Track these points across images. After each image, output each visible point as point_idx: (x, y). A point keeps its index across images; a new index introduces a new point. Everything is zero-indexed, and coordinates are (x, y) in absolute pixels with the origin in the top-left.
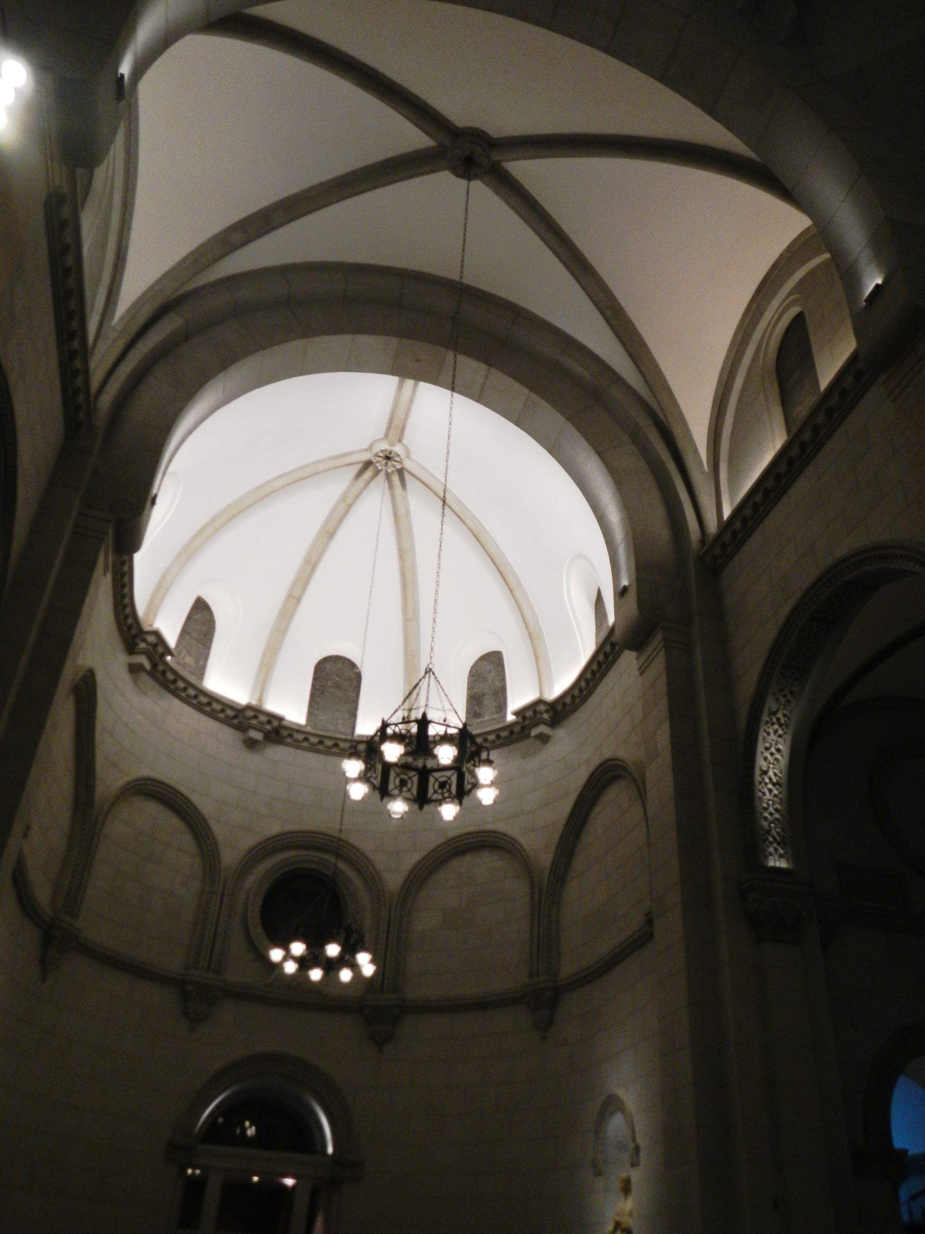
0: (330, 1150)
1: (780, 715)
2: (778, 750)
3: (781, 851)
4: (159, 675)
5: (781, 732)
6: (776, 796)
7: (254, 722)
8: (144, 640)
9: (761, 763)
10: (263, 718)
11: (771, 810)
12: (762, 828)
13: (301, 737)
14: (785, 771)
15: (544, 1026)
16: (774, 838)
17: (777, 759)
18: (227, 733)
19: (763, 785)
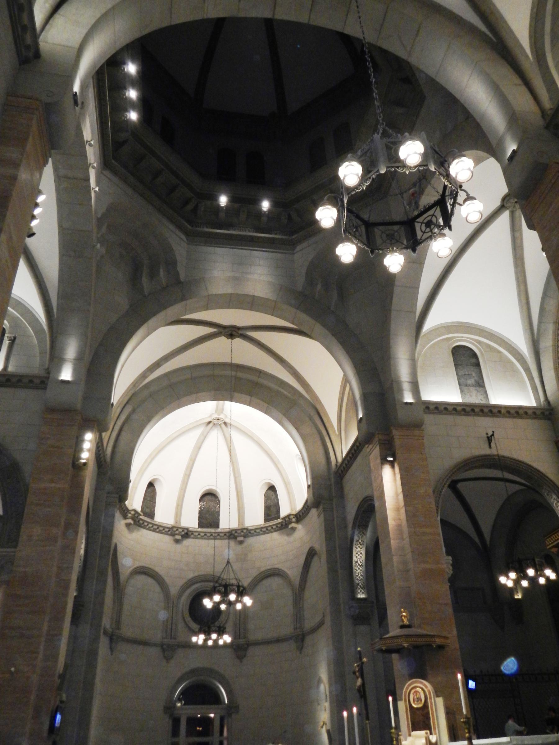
0: (226, 702)
1: (360, 541)
2: (361, 553)
3: (363, 591)
4: (138, 523)
5: (361, 547)
6: (361, 570)
7: (177, 532)
8: (130, 513)
9: (354, 559)
10: (180, 530)
11: (359, 575)
12: (356, 583)
13: (197, 534)
14: (364, 560)
15: (300, 649)
16: (360, 586)
17: (361, 557)
18: (167, 539)
19: (356, 567)
